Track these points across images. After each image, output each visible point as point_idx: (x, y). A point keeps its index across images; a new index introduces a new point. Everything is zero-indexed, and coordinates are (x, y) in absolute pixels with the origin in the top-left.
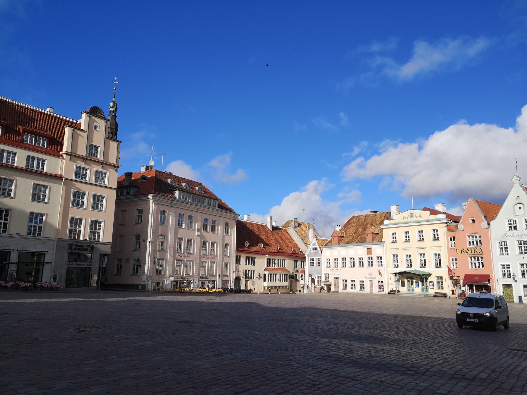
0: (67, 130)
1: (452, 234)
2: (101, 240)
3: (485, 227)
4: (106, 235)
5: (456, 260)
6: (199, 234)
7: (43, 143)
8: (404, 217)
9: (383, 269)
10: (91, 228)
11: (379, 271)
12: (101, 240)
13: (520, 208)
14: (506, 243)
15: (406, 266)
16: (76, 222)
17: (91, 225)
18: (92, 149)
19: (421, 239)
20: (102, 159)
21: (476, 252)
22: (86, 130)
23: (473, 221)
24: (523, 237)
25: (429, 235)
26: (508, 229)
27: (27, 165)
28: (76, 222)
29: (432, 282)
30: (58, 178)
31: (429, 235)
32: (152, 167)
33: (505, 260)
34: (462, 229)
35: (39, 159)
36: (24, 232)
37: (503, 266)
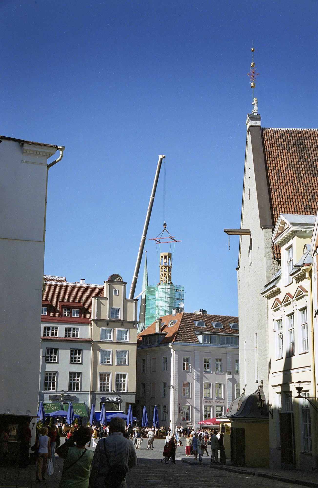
0: (93, 299)
2: (126, 391)
4: (130, 385)
6: (231, 377)
7: (76, 315)
10: (117, 381)
12: (126, 391)
16: (104, 376)
17: (117, 378)
18: (113, 312)
20: (122, 319)
22: (108, 297)
27: (66, 336)
28: (104, 376)
30: (88, 342)
32: (182, 309)
35: (74, 329)
36: (66, 389)
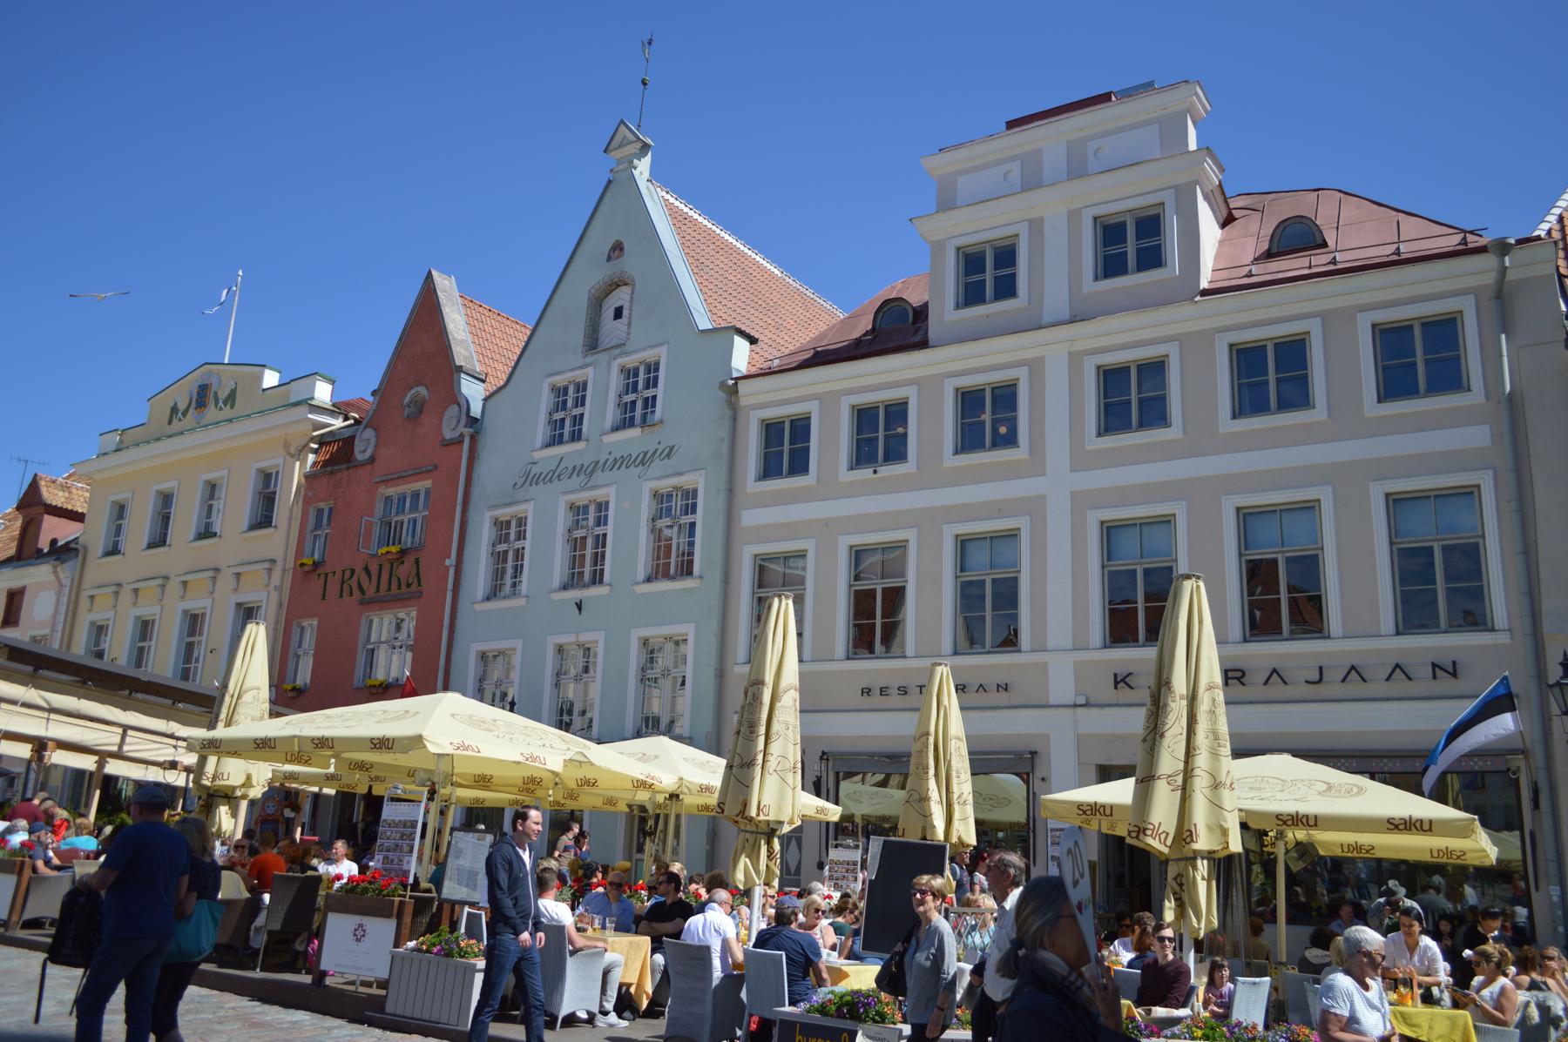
3: (456, 434)
13: (618, 313)
24: (599, 477)
26: (541, 432)
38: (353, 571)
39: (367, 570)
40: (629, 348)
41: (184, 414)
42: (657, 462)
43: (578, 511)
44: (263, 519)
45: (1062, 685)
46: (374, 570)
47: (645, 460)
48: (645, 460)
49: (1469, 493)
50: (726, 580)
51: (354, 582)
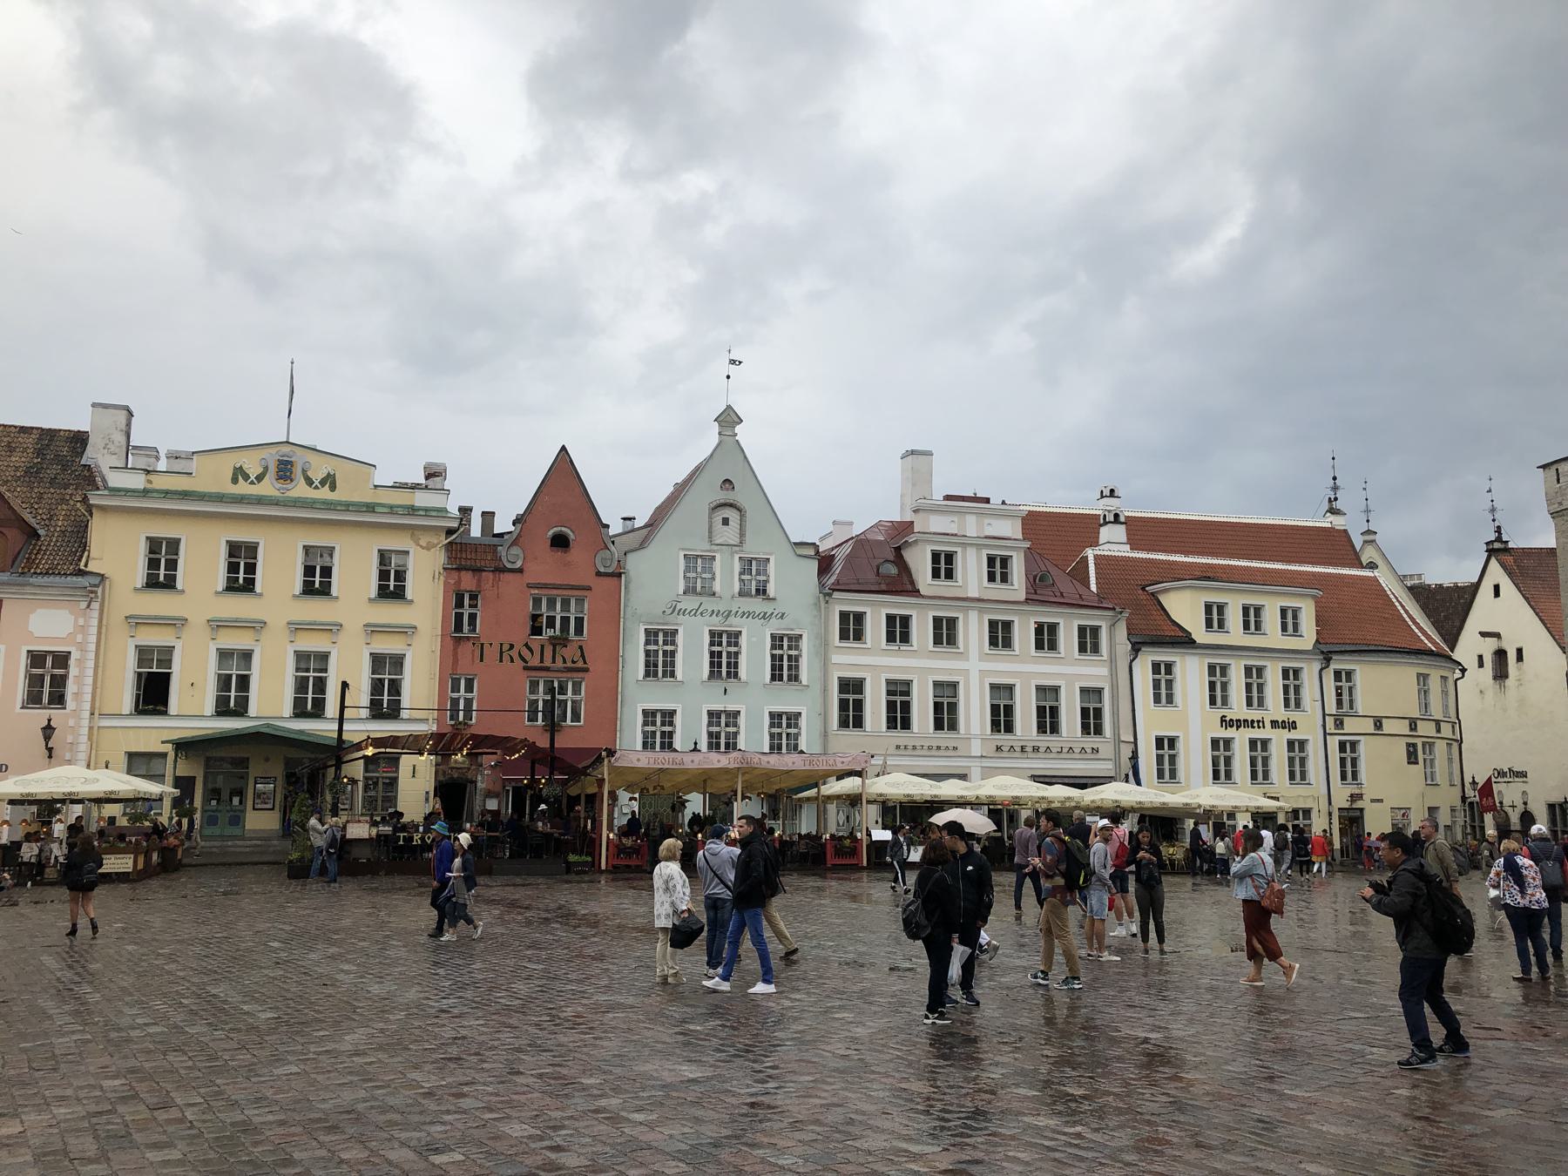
1: (468, 581)
5: (469, 689)
8: (239, 474)
9: (73, 717)
11: (48, 731)
13: (726, 522)
14: (671, 636)
15: (209, 708)
19: (317, 581)
21: (559, 660)
23: (560, 542)
24: (732, 620)
25: (355, 571)
29: (353, 782)
31: (355, 571)
33: (657, 697)
34: (519, 564)
37: (649, 715)
38: (512, 646)
39: (526, 645)
40: (746, 547)
41: (260, 478)
42: (773, 620)
43: (715, 637)
44: (391, 587)
45: (976, 748)
46: (536, 648)
47: (765, 616)
48: (765, 616)
49: (1099, 691)
50: (825, 690)
51: (514, 653)
